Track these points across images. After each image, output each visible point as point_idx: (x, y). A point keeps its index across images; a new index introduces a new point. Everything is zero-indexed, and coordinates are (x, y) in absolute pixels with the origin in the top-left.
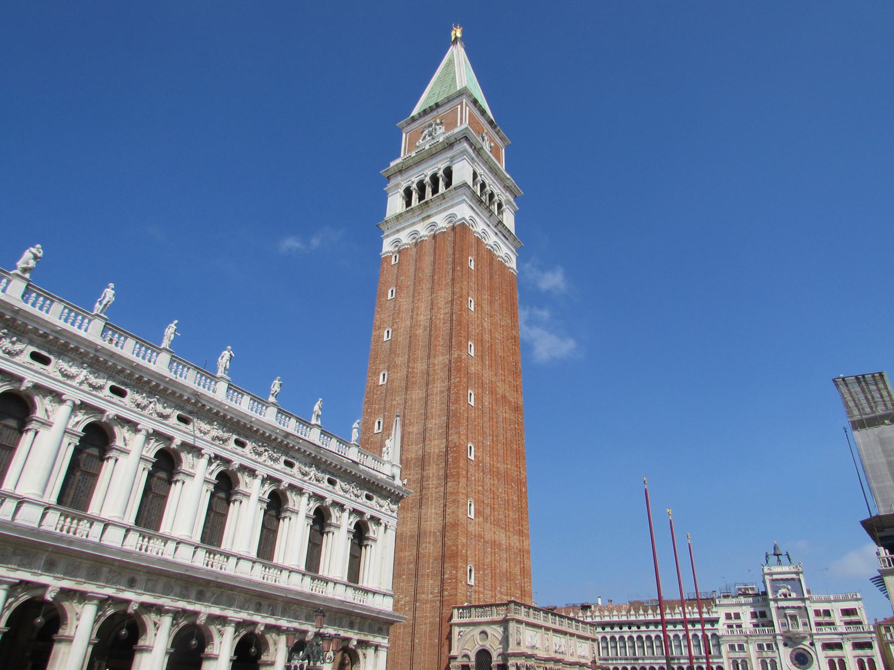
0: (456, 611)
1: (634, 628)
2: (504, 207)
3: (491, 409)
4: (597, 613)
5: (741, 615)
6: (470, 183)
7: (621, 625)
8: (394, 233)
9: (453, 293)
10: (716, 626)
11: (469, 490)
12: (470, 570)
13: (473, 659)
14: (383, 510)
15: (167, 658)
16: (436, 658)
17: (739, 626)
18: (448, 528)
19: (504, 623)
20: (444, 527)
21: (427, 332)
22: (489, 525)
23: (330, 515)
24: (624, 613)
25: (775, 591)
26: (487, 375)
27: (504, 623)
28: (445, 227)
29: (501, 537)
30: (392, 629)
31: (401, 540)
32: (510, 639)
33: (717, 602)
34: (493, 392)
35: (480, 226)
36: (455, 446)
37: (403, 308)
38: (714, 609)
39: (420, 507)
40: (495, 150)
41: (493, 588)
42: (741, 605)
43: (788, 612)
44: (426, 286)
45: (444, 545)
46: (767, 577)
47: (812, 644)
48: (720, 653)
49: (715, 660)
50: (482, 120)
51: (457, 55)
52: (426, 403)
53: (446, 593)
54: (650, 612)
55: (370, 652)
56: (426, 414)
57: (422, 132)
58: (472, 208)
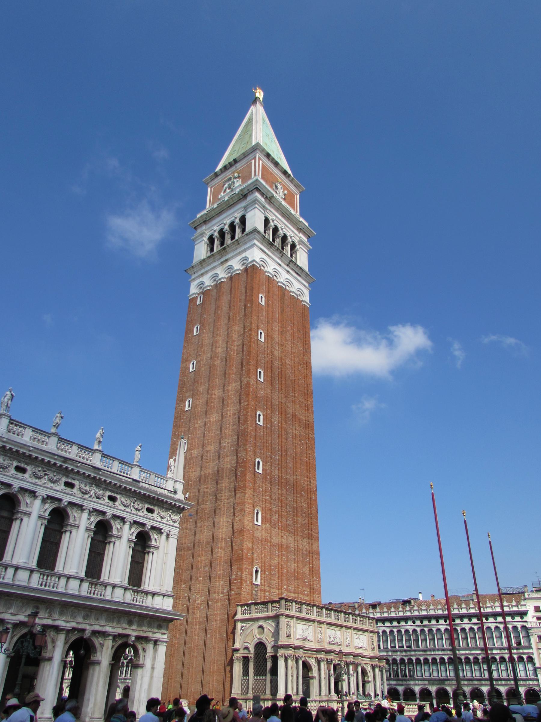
4: (416, 608)
6: (261, 229)
8: (199, 276)
9: (245, 327)
10: (525, 618)
11: (256, 499)
13: (252, 651)
14: (164, 521)
15: (9, 660)
16: (224, 650)
18: (235, 535)
19: (276, 618)
21: (224, 362)
22: (276, 530)
23: (111, 528)
26: (276, 398)
27: (276, 618)
28: (240, 269)
29: (289, 540)
30: (171, 625)
31: (199, 547)
32: (280, 632)
33: (526, 596)
34: (282, 412)
35: (273, 266)
36: (243, 462)
38: (523, 603)
39: (215, 517)
40: (289, 198)
41: (280, 587)
44: (223, 322)
48: (530, 643)
49: (526, 651)
50: (276, 171)
51: (258, 113)
52: (221, 425)
53: (233, 592)
54: (463, 606)
55: (150, 646)
58: (263, 251)
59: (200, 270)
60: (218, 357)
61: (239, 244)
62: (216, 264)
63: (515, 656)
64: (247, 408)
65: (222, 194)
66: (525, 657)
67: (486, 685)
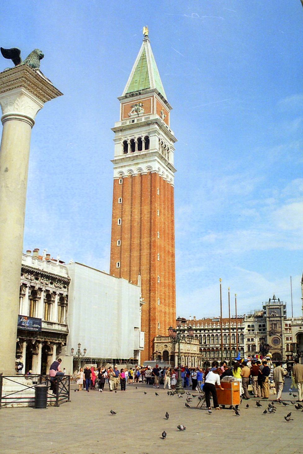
0: (155, 338)
1: (207, 332)
2: (170, 150)
3: (165, 259)
5: (255, 326)
7: (200, 330)
8: (120, 167)
9: (151, 208)
12: (159, 324)
13: (162, 354)
33: (245, 321)
36: (154, 278)
37: (127, 210)
44: (137, 201)
45: (150, 315)
49: (241, 345)
53: (151, 332)
56: (140, 263)
57: (132, 107)
58: (159, 162)
59: (120, 162)
60: (136, 221)
61: (146, 156)
62: (131, 163)
64: (155, 254)
65: (131, 113)
66: (240, 348)
67: (220, 360)
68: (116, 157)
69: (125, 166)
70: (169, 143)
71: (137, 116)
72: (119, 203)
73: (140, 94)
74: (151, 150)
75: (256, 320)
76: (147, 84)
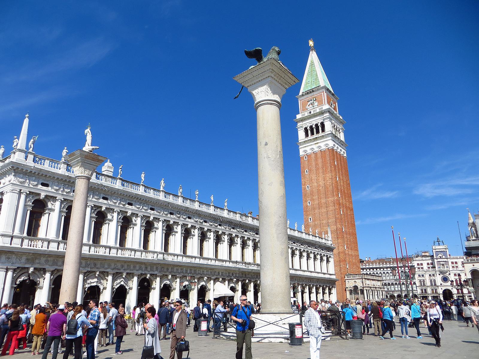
0: (346, 276)
1: (382, 270)
2: (341, 131)
7: (377, 268)
17: (422, 268)
20: (339, 253)
24: (378, 264)
25: (437, 255)
33: (414, 260)
42: (423, 260)
43: (441, 263)
44: (321, 171)
46: (434, 251)
47: (449, 274)
50: (330, 95)
51: (313, 57)
54: (388, 263)
59: (304, 144)
63: (409, 282)
65: (308, 106)
68: (300, 140)
69: (307, 146)
70: (340, 127)
71: (313, 108)
72: (306, 173)
73: (313, 91)
74: (327, 132)
75: (424, 259)
76: (318, 83)
